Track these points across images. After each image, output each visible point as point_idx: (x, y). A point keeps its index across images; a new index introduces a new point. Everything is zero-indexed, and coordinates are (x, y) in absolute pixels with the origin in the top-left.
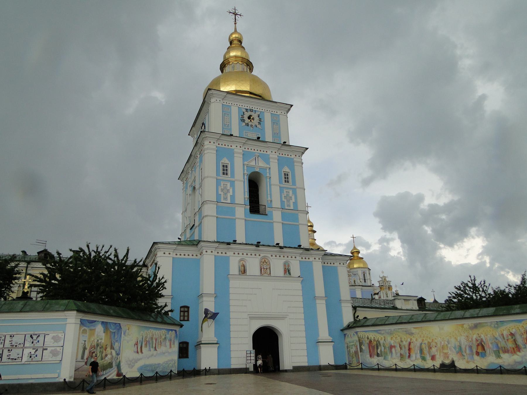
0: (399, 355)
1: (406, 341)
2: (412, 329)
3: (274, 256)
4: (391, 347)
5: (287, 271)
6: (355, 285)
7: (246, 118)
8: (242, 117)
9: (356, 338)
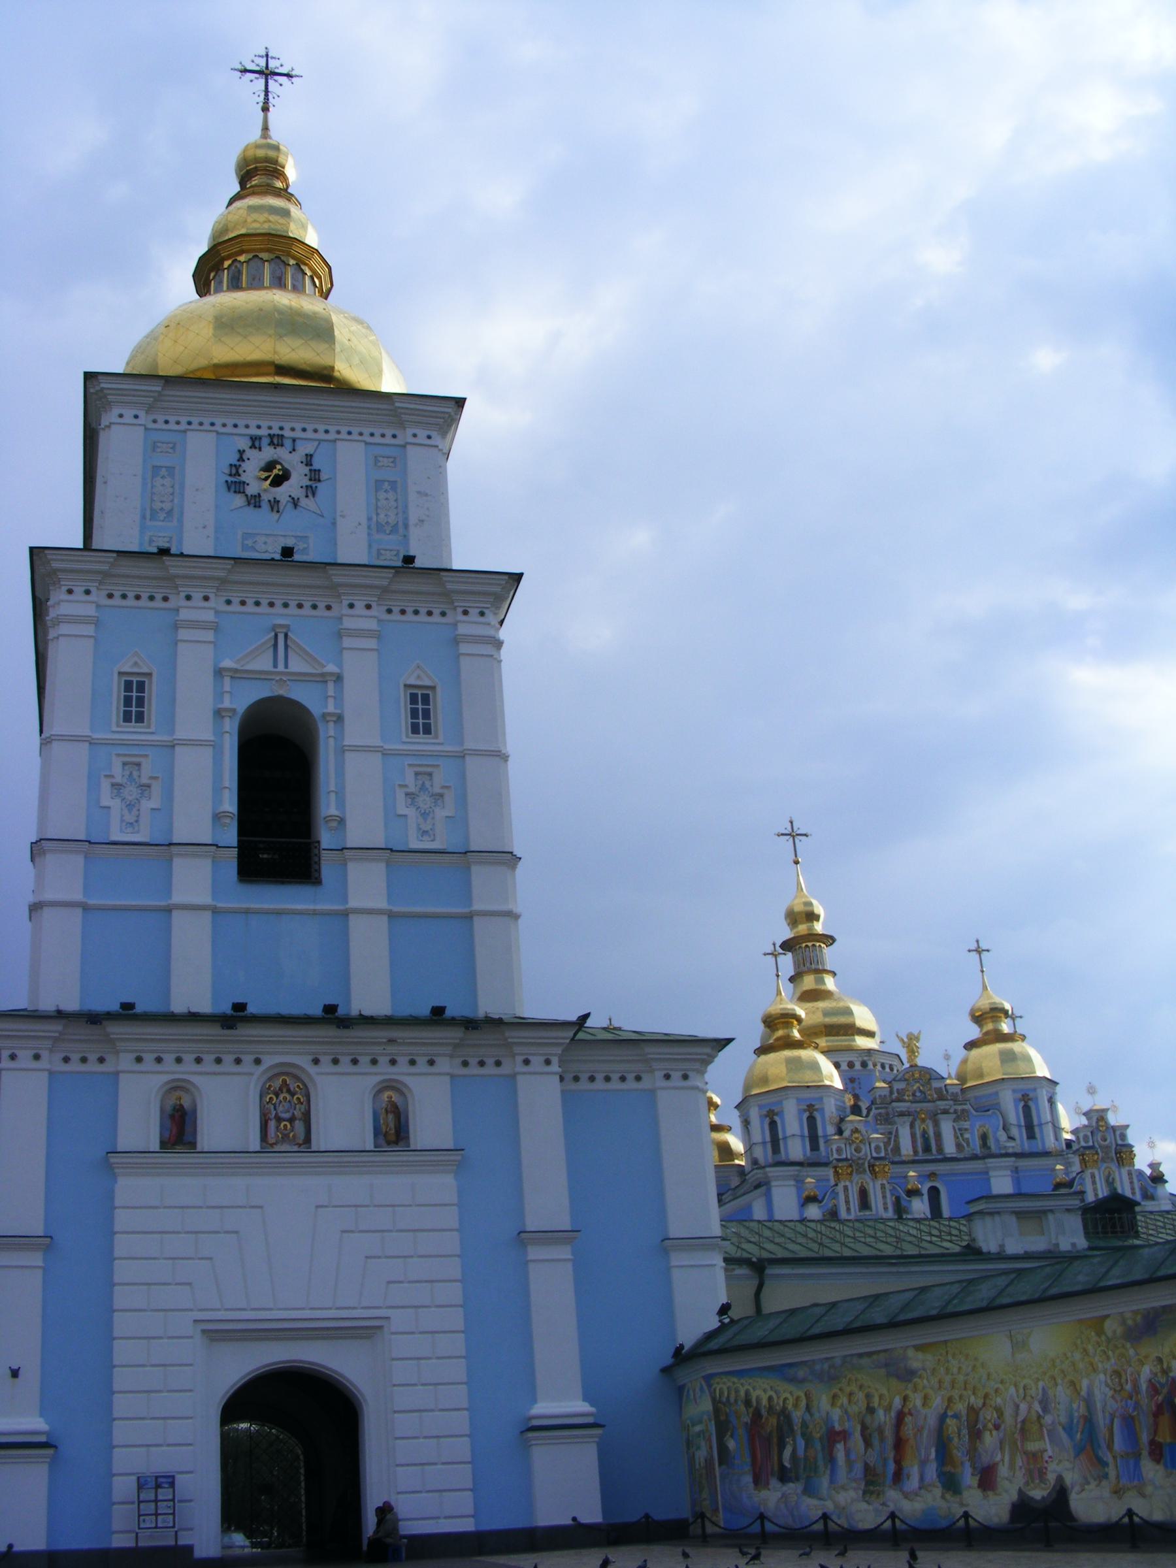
0: (859, 1467)
1: (888, 1409)
2: (911, 1353)
3: (325, 1060)
4: (834, 1437)
6: (986, 1152)
7: (251, 471)
8: (234, 471)
9: (706, 1405)
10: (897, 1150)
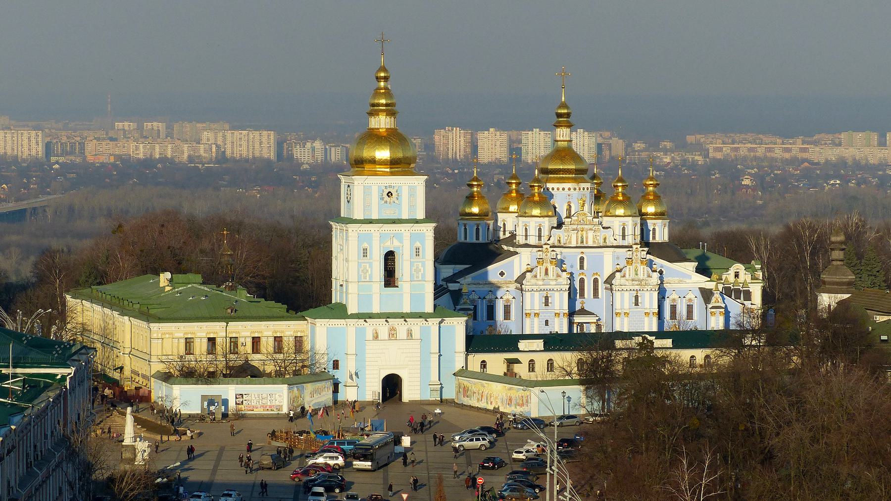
4: (474, 393)
5: (410, 334)
6: (605, 244)
10: (570, 242)
